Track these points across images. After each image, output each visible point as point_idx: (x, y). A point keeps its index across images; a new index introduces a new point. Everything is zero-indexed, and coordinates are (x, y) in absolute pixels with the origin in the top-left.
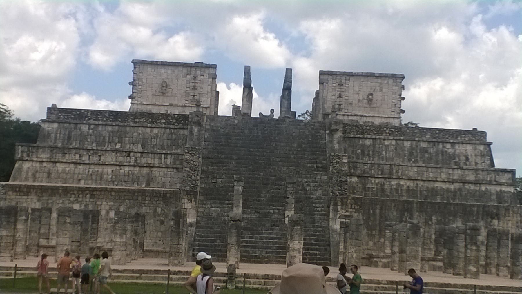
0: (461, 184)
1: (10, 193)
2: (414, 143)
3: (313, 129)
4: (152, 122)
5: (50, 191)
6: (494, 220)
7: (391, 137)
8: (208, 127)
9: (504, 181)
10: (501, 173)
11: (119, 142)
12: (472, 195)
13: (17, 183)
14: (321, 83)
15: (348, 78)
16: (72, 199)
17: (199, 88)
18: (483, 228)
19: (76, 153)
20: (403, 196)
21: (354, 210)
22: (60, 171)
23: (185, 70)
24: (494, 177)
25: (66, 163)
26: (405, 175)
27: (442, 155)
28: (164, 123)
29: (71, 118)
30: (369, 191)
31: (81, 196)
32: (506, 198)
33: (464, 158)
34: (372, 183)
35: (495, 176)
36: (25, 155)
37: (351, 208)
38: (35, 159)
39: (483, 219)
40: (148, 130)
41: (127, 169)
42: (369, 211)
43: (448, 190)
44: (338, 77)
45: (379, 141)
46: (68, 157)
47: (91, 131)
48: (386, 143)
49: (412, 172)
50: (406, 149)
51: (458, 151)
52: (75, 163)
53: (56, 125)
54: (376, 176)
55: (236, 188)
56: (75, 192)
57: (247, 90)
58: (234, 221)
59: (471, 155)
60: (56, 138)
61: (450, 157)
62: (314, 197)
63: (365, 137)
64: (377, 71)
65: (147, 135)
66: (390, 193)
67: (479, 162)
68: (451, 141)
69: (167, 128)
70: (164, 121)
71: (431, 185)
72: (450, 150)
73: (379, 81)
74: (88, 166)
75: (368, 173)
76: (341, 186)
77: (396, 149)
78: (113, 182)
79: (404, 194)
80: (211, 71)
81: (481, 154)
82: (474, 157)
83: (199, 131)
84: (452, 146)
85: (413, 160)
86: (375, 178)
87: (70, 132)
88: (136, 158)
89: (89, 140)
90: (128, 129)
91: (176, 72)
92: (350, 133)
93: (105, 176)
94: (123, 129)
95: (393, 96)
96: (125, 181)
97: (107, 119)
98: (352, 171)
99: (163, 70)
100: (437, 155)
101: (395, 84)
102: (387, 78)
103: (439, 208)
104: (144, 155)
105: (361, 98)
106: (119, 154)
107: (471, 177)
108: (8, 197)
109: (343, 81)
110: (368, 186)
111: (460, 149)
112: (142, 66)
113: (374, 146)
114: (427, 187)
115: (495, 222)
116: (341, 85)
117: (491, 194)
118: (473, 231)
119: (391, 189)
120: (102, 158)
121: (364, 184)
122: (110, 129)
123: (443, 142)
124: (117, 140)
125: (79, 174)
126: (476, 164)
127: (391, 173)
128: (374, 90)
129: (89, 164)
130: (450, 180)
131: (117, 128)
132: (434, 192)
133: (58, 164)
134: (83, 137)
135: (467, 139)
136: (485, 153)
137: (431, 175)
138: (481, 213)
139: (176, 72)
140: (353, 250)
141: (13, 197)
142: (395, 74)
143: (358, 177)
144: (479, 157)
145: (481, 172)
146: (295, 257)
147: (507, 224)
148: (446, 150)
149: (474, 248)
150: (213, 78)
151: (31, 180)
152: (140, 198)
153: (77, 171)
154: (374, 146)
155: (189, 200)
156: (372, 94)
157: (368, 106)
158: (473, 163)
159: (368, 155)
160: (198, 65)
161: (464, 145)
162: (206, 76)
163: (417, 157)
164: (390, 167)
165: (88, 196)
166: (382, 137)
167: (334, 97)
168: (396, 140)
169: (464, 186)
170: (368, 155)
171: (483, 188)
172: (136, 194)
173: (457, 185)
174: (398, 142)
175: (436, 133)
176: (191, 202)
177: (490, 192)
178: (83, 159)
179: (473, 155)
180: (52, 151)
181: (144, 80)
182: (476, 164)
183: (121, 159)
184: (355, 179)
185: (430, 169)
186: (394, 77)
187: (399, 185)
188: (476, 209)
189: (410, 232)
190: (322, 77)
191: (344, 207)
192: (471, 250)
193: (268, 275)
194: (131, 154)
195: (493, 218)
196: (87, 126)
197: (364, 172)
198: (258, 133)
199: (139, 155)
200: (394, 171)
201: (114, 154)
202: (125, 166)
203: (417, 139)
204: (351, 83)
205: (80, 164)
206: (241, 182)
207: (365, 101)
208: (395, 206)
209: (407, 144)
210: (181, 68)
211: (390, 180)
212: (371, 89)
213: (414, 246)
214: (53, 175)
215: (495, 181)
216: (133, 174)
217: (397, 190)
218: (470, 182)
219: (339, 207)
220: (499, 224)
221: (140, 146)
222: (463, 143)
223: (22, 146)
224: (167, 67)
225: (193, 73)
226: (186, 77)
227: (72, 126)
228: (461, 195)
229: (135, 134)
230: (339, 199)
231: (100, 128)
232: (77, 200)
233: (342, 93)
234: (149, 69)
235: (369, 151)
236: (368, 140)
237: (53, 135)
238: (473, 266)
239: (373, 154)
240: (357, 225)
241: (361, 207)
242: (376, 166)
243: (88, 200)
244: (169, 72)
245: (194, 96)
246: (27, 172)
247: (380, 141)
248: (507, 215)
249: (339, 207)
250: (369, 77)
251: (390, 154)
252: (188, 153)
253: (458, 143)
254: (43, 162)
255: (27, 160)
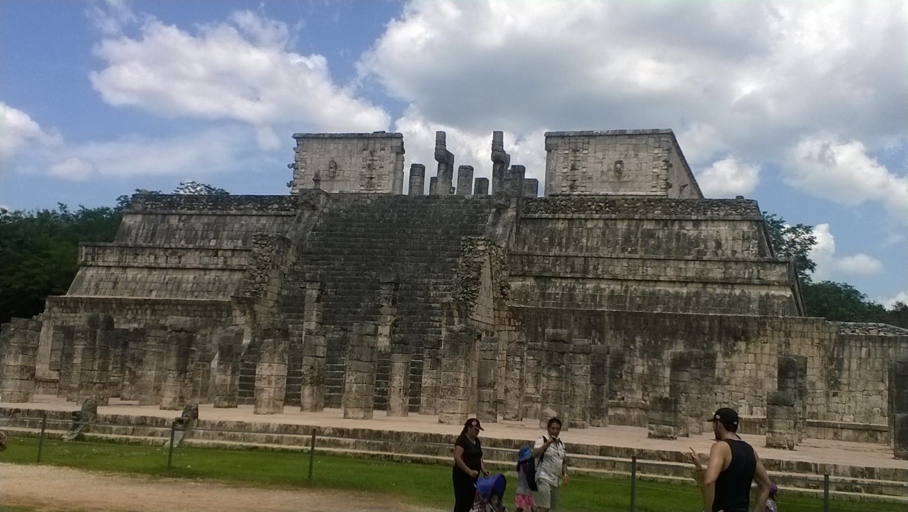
0: (700, 286)
1: (55, 309)
2: (634, 222)
3: (475, 207)
4: (261, 209)
5: (101, 306)
6: (739, 343)
7: (597, 216)
8: (326, 210)
9: (773, 279)
10: (768, 266)
11: (214, 238)
12: (717, 303)
13: (76, 296)
14: (548, 149)
15: (586, 140)
16: (129, 317)
17: (378, 168)
18: (719, 355)
19: (150, 254)
20: (601, 306)
21: (514, 328)
22: (129, 279)
23: (361, 144)
24: (755, 271)
25: (138, 267)
26: (607, 272)
27: (678, 240)
28: (277, 209)
29: (160, 207)
30: (549, 298)
31: (139, 312)
32: (776, 307)
33: (714, 244)
34: (556, 287)
35: (758, 271)
36: (89, 258)
37: (509, 325)
38: (101, 264)
39: (720, 341)
40: (254, 220)
41: (213, 274)
42: (536, 328)
43: (677, 296)
44: (573, 140)
45: (578, 222)
46: (142, 260)
47: (181, 224)
48: (590, 225)
49: (619, 269)
50: (620, 234)
51: (704, 233)
52: (150, 268)
53: (139, 218)
54: (562, 275)
55: (308, 292)
56: (133, 307)
57: (443, 167)
58: (176, 331)
59: (727, 239)
60: (137, 235)
61: (690, 243)
62: (437, 305)
63: (557, 216)
64: (630, 128)
65: (252, 226)
66: (583, 301)
67: (739, 250)
68: (694, 217)
69: (279, 216)
70: (276, 206)
71: (648, 289)
72: (691, 233)
73: (634, 141)
74: (165, 272)
75: (550, 270)
76: (466, 287)
77: (604, 234)
78: (192, 292)
79: (605, 303)
80: (395, 143)
81: (743, 236)
82: (731, 242)
83: (310, 216)
84: (694, 225)
85: (629, 249)
86: (562, 278)
87: (155, 227)
88: (225, 258)
89: (177, 237)
90: (228, 218)
91: (349, 147)
92: (535, 212)
93: (184, 285)
94: (221, 220)
95: (655, 163)
96: (208, 291)
97: (205, 206)
98: (526, 268)
99: (332, 146)
100: (669, 238)
101: (657, 145)
102: (646, 137)
103: (646, 323)
104: (236, 254)
105: (605, 170)
106: (203, 254)
107: (717, 273)
108: (53, 315)
109: (580, 145)
110: (549, 291)
111: (707, 230)
112: (305, 142)
113: (570, 230)
114: (644, 292)
115: (742, 345)
116: (575, 151)
117: (750, 301)
118: (554, 343)
119: (584, 296)
120: (183, 259)
121: (543, 289)
122: (205, 220)
123: (680, 221)
124: (212, 235)
125: (152, 282)
126: (734, 252)
127: (585, 271)
128: (626, 155)
129: (165, 268)
130: (681, 279)
131: (214, 218)
132: (654, 299)
133: (128, 270)
134: (170, 233)
135: (722, 214)
136: (751, 234)
137: (650, 271)
138: (717, 329)
139: (349, 147)
140: (351, 377)
141: (59, 315)
142: (658, 130)
143: (536, 278)
144: (741, 242)
145: (734, 266)
146: (262, 390)
147: (762, 348)
148: (685, 232)
149: (554, 374)
150: (397, 153)
151: (92, 291)
152: (214, 314)
153: (150, 279)
154: (570, 230)
155: (242, 312)
156: (620, 162)
157: (616, 180)
158: (729, 252)
159: (560, 244)
160: (378, 136)
161: (716, 223)
162: (388, 148)
163: (636, 244)
164: (585, 261)
165: (148, 312)
166: (583, 216)
167: (565, 170)
168: (605, 220)
169: (704, 288)
170: (560, 244)
171: (737, 292)
172: (209, 308)
173: (693, 288)
174: (609, 222)
175: (672, 207)
176: (245, 315)
177: (749, 298)
178: (159, 261)
179: (730, 238)
180: (121, 252)
181: (308, 161)
182: (734, 252)
183: (206, 260)
184: (530, 282)
185: (648, 262)
186: (655, 134)
187: (597, 289)
188: (707, 323)
189: (448, 346)
190: (549, 142)
191: (463, 319)
192: (549, 377)
193: (145, 418)
194: (220, 253)
195: (737, 339)
196: (177, 217)
197: (544, 270)
198: (393, 216)
199: (229, 254)
200: (591, 267)
201: (197, 253)
202: (211, 269)
203: (637, 217)
204: (591, 148)
205: (155, 268)
206: (315, 284)
207: (612, 173)
208: (575, 321)
209: (622, 226)
210: (355, 142)
211: (585, 281)
212: (622, 154)
213: (452, 370)
214: (119, 285)
215: (759, 279)
216: (220, 281)
217: (594, 297)
218: (715, 282)
219: (456, 320)
220: (747, 348)
221: (240, 242)
222: (713, 221)
223: (86, 247)
224: (337, 141)
225: (371, 147)
226: (361, 153)
227: (160, 218)
228: (697, 301)
229: (237, 226)
230: (455, 307)
231: (193, 221)
232: (135, 318)
233: (578, 163)
234: (315, 145)
235: (562, 238)
236: (561, 221)
237: (134, 232)
238: (553, 408)
239: (568, 242)
240: (360, 335)
241: (523, 323)
242: (563, 259)
243: (148, 317)
244: (341, 147)
245: (371, 178)
246: (90, 282)
247: (581, 223)
248: (761, 333)
249: (456, 320)
250: (619, 137)
251: (593, 242)
252: (256, 243)
253: (706, 220)
254: (111, 267)
255: (91, 266)
